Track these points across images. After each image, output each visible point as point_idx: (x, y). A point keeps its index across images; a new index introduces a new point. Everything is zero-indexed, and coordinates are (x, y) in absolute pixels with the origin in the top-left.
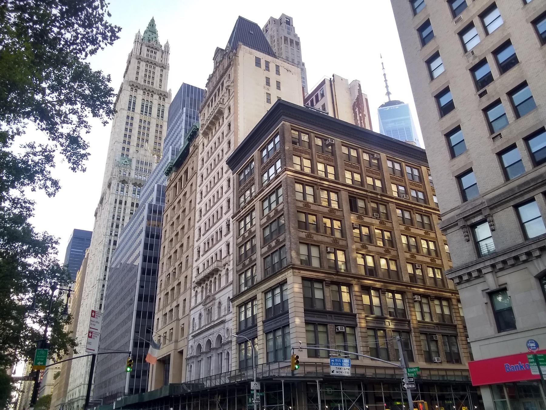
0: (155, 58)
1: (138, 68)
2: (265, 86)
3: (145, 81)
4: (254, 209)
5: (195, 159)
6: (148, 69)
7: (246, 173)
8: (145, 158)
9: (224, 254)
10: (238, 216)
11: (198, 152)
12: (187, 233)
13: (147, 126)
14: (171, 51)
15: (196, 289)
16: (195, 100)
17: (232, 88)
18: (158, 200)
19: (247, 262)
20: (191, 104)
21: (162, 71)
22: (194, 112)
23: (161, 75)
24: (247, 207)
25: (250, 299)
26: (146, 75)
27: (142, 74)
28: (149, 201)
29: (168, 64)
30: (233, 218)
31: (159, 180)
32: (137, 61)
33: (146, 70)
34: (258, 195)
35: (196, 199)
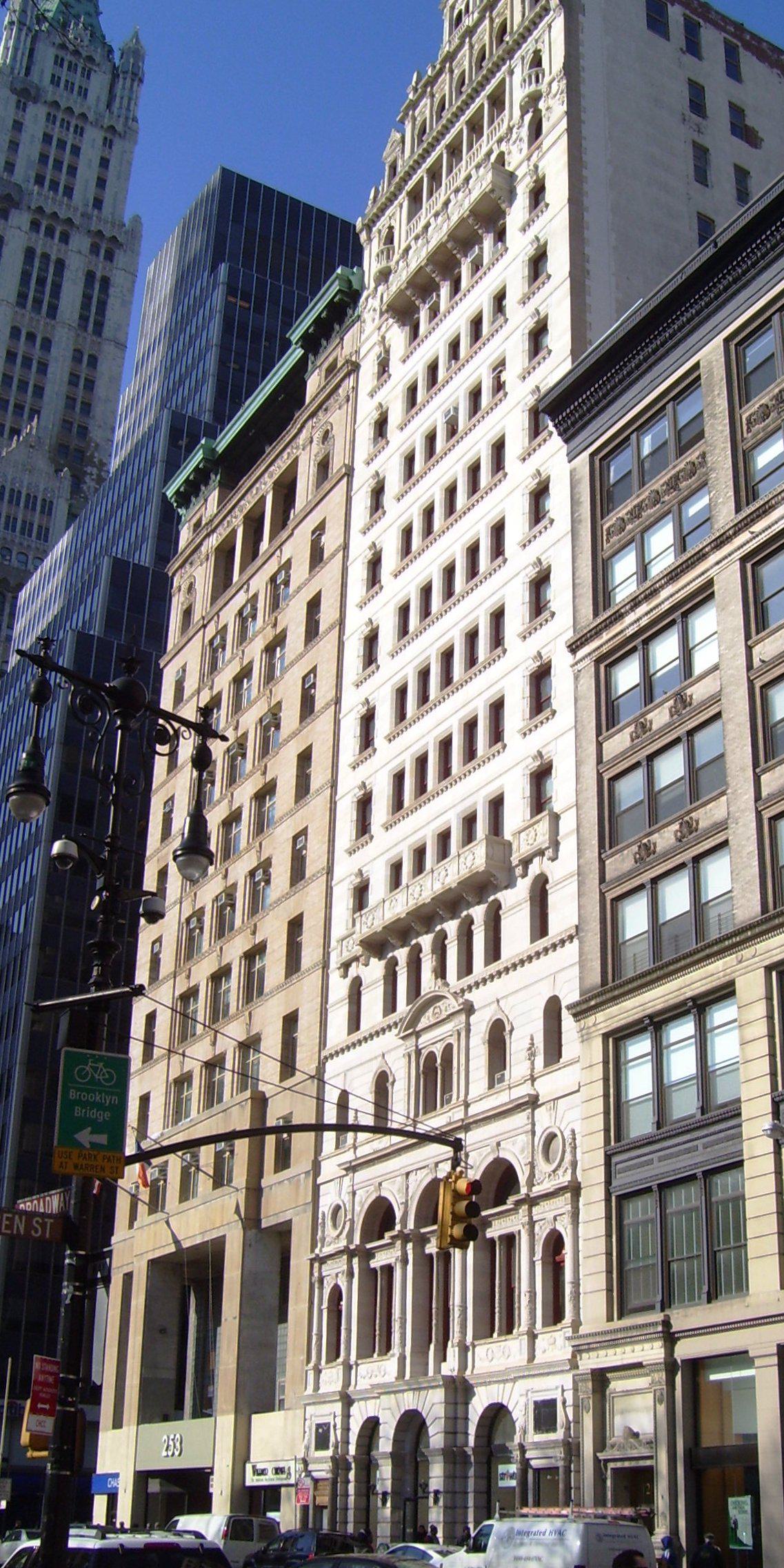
0: (84, 93)
1: (18, 126)
2: (688, 112)
3: (40, 180)
4: (712, 595)
5: (336, 418)
6: (56, 133)
7: (646, 450)
8: (26, 479)
9: (516, 813)
10: (605, 636)
11: (355, 389)
12: (294, 735)
13: (37, 352)
14: (149, 67)
15: (353, 971)
16: (264, 239)
17: (551, 102)
18: (112, 619)
19: (665, 838)
20: (248, 255)
21: (108, 143)
22: (262, 284)
23: (104, 163)
24: (664, 594)
25: (693, 999)
26: (44, 158)
27: (30, 149)
28: (78, 621)
29: (135, 120)
30: (573, 648)
31: (118, 535)
32: (14, 98)
33: (47, 138)
34: (736, 534)
35: (344, 585)
